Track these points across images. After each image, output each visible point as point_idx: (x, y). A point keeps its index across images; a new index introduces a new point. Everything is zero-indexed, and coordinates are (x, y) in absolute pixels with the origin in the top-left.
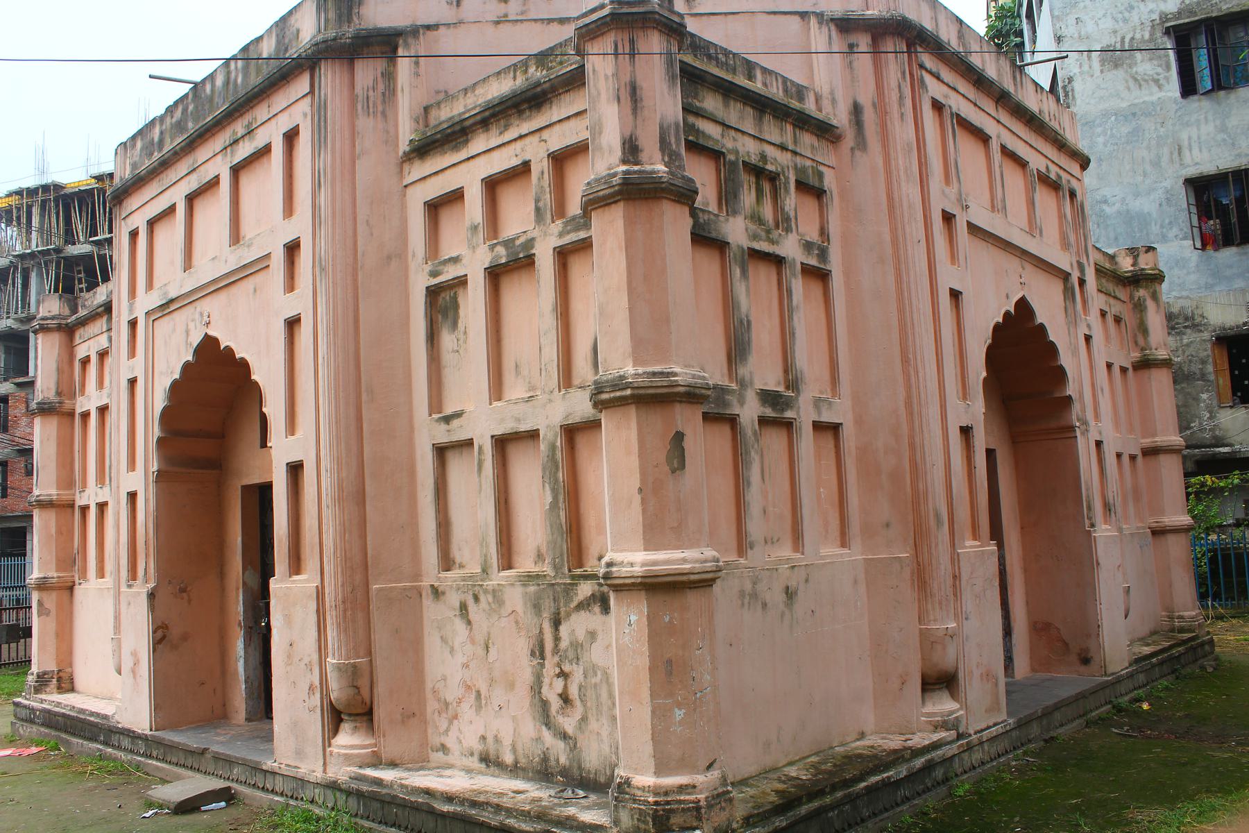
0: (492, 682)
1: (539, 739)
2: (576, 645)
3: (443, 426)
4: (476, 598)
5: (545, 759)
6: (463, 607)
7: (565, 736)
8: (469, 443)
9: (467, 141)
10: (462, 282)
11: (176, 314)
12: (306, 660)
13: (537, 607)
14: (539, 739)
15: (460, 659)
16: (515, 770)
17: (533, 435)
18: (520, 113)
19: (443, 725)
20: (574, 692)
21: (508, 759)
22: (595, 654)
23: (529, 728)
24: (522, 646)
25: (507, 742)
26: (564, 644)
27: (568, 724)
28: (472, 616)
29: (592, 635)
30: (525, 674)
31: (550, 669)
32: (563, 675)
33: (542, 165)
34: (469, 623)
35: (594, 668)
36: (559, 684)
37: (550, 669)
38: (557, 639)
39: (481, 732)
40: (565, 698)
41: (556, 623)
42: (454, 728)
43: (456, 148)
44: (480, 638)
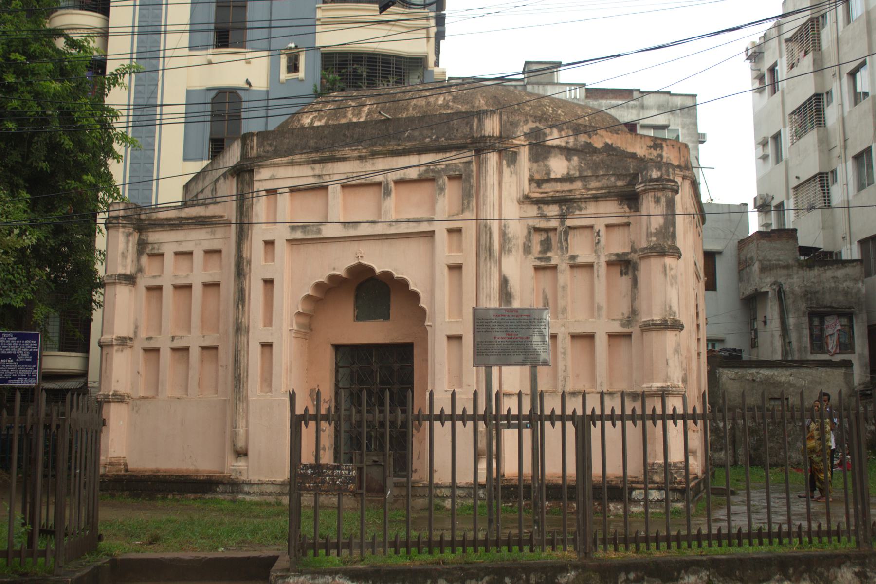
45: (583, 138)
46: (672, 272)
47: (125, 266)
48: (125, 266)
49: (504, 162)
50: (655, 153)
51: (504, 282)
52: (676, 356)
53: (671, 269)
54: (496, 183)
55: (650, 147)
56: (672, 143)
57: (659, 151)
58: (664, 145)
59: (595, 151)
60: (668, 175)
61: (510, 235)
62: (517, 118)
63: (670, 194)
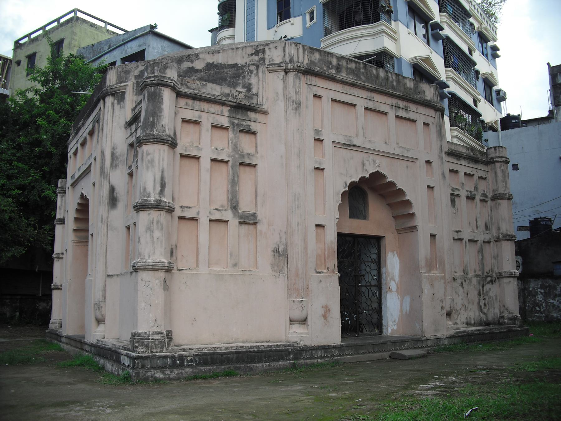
0: (469, 303)
1: (479, 316)
2: (487, 292)
3: (456, 233)
4: (465, 281)
5: (481, 320)
6: (462, 283)
7: (485, 314)
8: (461, 240)
9: (460, 160)
10: (459, 196)
11: (352, 152)
12: (440, 299)
13: (479, 283)
14: (479, 316)
15: (461, 297)
16: (474, 325)
17: (476, 241)
18: (472, 161)
19: (456, 317)
20: (486, 302)
21: (473, 322)
22: (491, 294)
23: (477, 313)
24: (476, 293)
25: (472, 318)
26: (485, 292)
27: (485, 311)
28: (464, 286)
29: (490, 289)
30: (476, 300)
31: (482, 298)
32: (484, 299)
33: (476, 177)
34: (463, 287)
35: (490, 296)
36: (484, 301)
37: (482, 298)
38: (483, 291)
39: (466, 316)
40: (485, 304)
41: (483, 287)
42: (459, 317)
43: (457, 159)
44: (466, 292)
45: (186, 65)
46: (149, 157)
47: (60, 214)
48: (60, 214)
49: (116, 101)
50: (256, 58)
51: (112, 190)
52: (148, 234)
53: (148, 154)
54: (110, 118)
55: (252, 55)
56: (275, 45)
57: (261, 55)
58: (267, 49)
59: (197, 71)
60: (153, 73)
61: (117, 154)
62: (130, 67)
63: (153, 89)
